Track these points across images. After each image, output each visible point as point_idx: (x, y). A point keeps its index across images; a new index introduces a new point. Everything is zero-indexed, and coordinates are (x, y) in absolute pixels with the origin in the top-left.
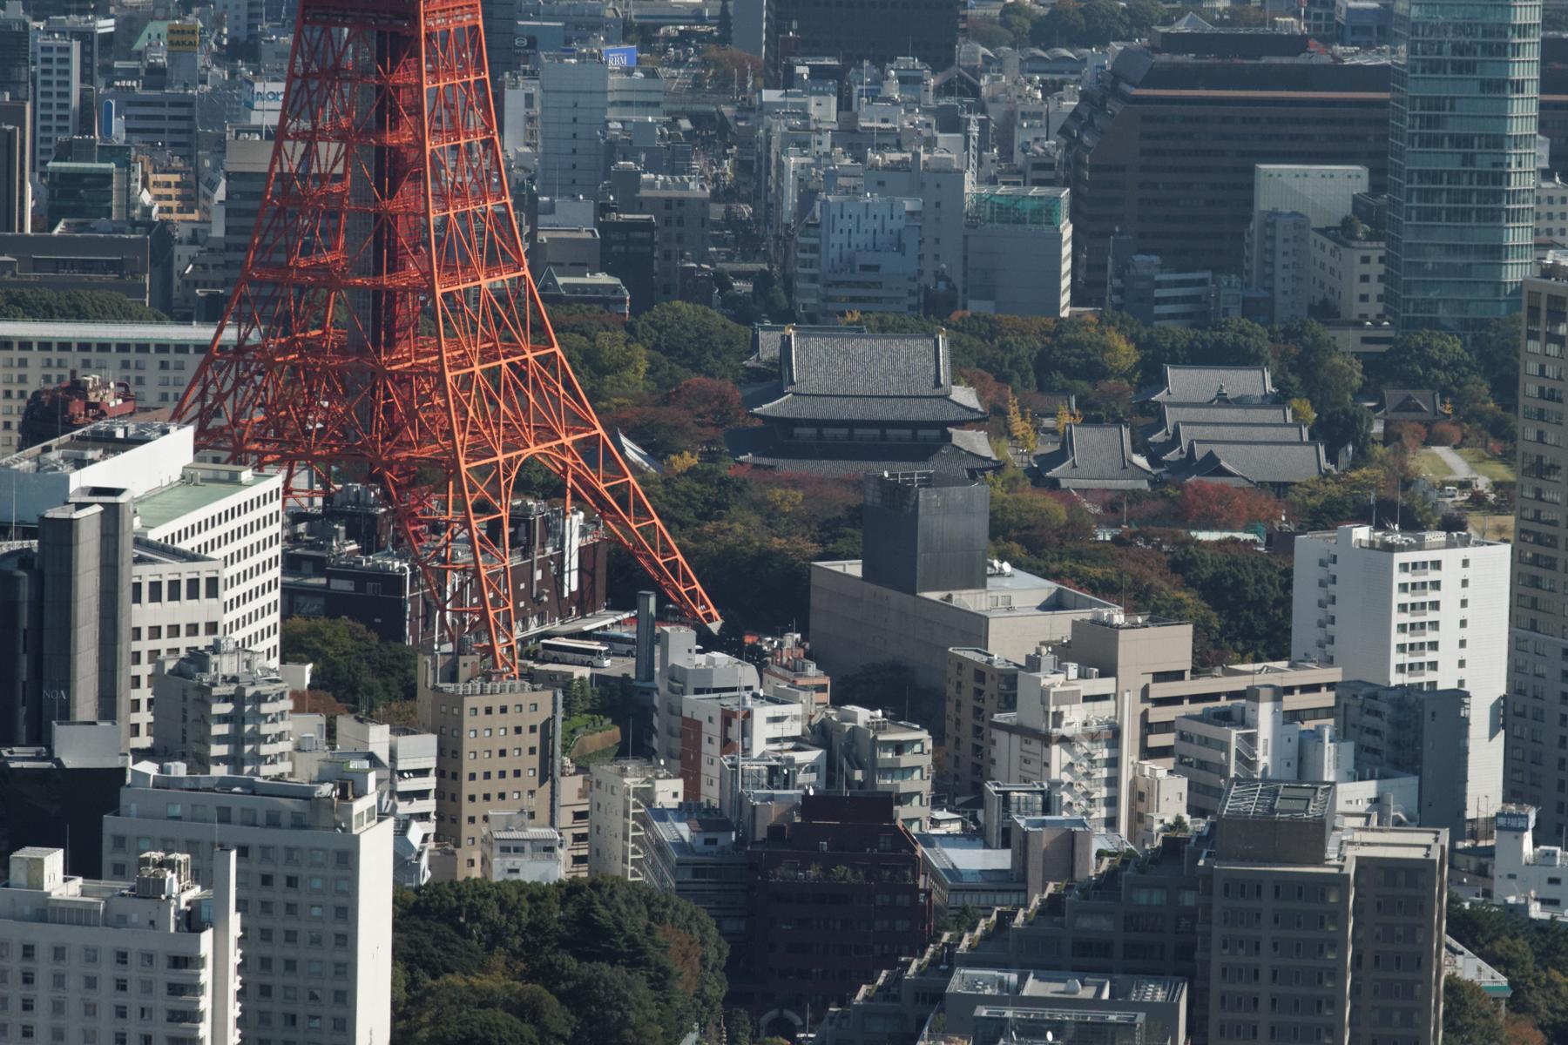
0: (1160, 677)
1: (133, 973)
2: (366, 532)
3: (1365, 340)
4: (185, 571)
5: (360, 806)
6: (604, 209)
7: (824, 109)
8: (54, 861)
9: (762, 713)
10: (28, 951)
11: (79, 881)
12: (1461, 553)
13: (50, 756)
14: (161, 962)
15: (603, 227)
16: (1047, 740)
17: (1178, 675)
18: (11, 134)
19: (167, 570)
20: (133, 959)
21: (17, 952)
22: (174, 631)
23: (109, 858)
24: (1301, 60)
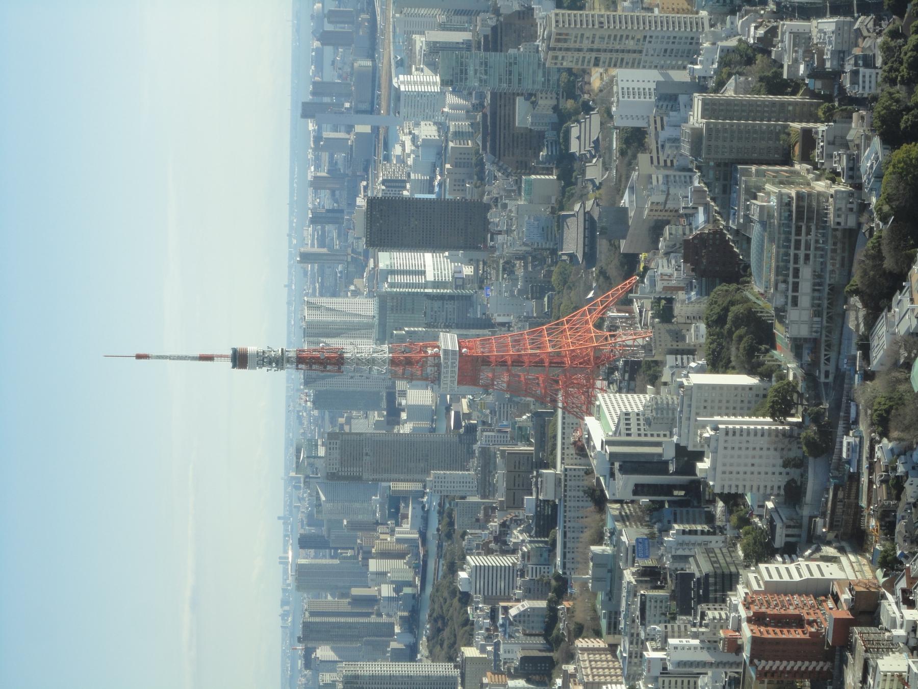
0: (652, 163)
1: (729, 445)
2: (612, 370)
3: (563, 98)
4: (623, 422)
5: (686, 383)
6: (527, 298)
7: (500, 238)
8: (700, 465)
9: (660, 270)
10: (724, 473)
11: (705, 459)
12: (619, 82)
13: (672, 460)
14: (727, 438)
15: (532, 298)
16: (668, 194)
17: (652, 157)
18: (508, 453)
19: (623, 427)
20: (726, 445)
21: (724, 475)
22: (639, 425)
23: (699, 449)
24: (488, 114)
